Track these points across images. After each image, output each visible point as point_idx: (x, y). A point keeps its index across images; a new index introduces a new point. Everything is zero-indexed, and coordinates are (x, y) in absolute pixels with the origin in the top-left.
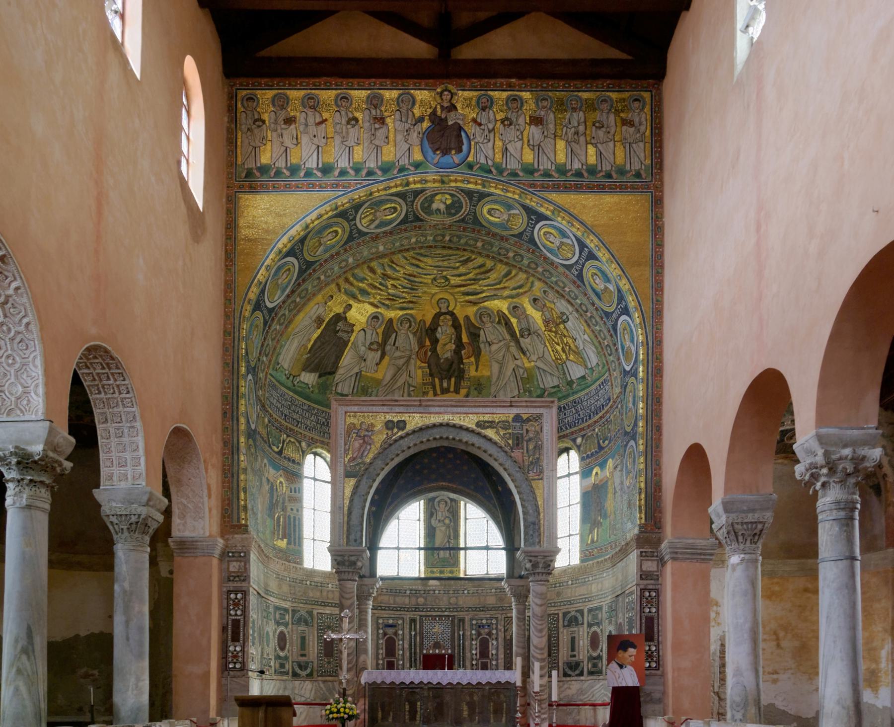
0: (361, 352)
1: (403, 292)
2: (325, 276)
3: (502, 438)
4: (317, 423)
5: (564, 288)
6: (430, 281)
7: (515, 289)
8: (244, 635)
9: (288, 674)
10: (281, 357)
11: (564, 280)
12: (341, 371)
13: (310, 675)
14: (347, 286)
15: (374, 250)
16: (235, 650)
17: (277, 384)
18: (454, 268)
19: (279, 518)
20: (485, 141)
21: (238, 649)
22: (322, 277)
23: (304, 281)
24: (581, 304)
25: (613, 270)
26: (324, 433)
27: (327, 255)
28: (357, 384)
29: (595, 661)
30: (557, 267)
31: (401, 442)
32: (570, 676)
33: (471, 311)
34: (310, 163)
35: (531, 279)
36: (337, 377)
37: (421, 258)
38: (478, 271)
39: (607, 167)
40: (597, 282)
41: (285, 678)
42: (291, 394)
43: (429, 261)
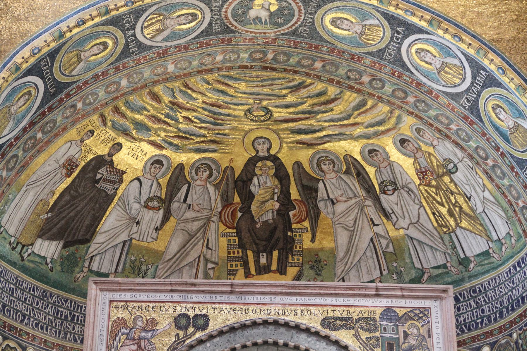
1: (201, 128)
2: (84, 104)
5: (449, 125)
6: (242, 114)
7: (372, 125)
11: (448, 113)
15: (160, 70)
22: (80, 105)
24: (477, 148)
30: (437, 97)
35: (397, 112)
37: (230, 83)
38: (316, 100)
40: (501, 117)
43: (243, 86)
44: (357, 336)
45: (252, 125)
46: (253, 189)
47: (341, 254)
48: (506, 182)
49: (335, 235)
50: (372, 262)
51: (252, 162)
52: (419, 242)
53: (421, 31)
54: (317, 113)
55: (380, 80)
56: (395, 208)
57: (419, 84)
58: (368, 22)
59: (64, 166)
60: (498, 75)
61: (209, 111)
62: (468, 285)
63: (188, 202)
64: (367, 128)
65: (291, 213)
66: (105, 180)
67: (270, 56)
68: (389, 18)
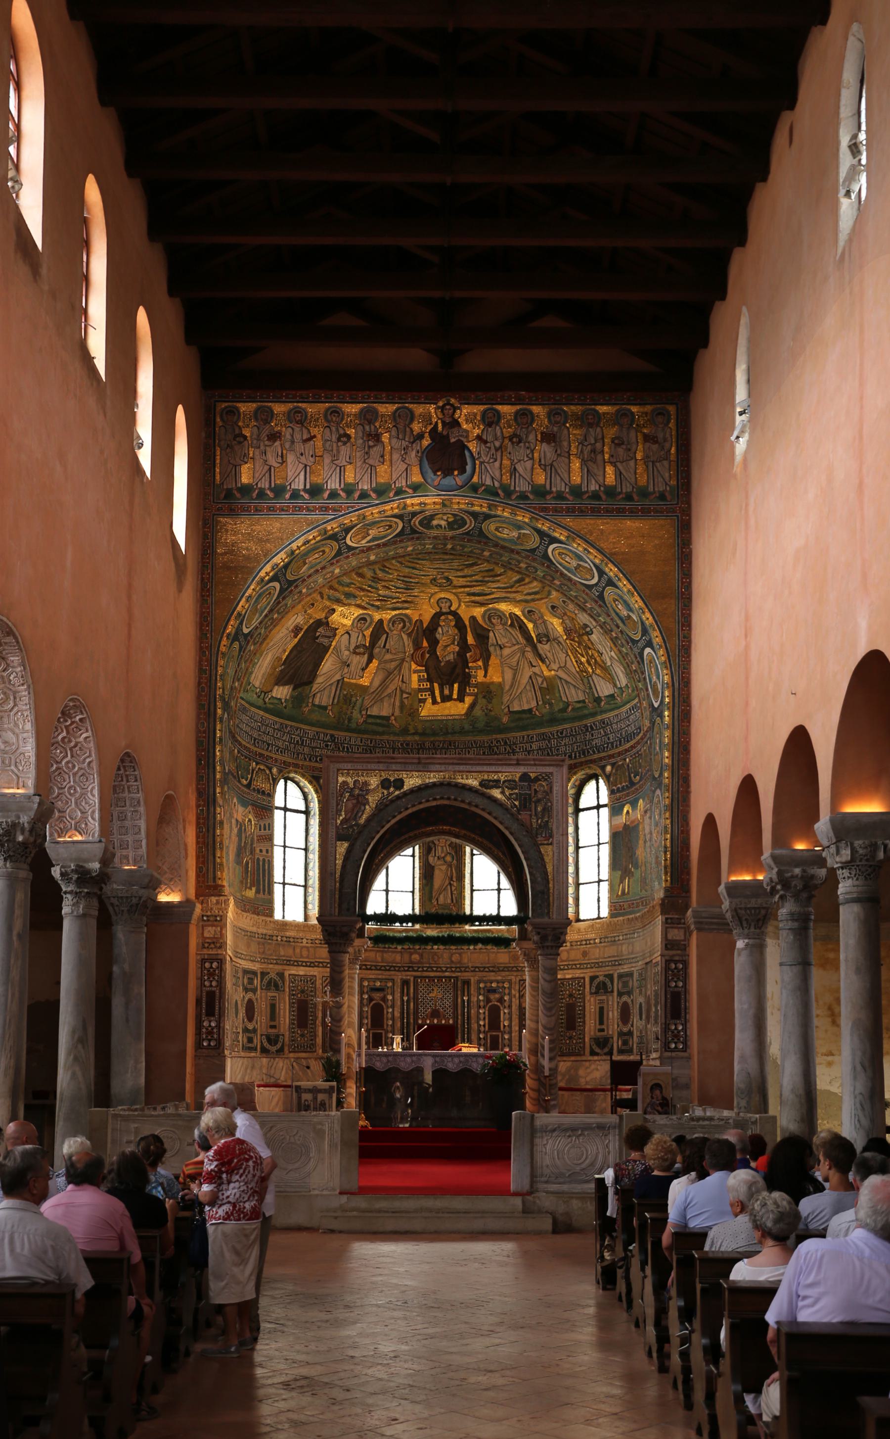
0: (344, 657)
3: (508, 799)
4: (290, 743)
8: (220, 1008)
9: (256, 1049)
10: (253, 675)
11: (584, 596)
12: (319, 680)
15: (364, 560)
16: (210, 1026)
17: (247, 705)
18: (457, 570)
19: (247, 863)
20: (492, 460)
21: (213, 1024)
23: (284, 599)
26: (298, 755)
27: (312, 570)
28: (338, 692)
29: (626, 1037)
31: (399, 802)
32: (597, 1054)
33: (478, 612)
34: (297, 484)
35: (547, 588)
36: (315, 686)
39: (627, 488)
41: (253, 1054)
42: (262, 713)
45: (436, 589)
46: (437, 636)
47: (507, 688)
50: (531, 694)
51: (437, 617)
52: (566, 682)
53: (560, 542)
54: (488, 582)
55: (534, 567)
56: (549, 655)
57: (562, 574)
59: (292, 631)
60: (615, 580)
61: (403, 581)
63: (387, 647)
64: (526, 595)
65: (468, 655)
66: (323, 636)
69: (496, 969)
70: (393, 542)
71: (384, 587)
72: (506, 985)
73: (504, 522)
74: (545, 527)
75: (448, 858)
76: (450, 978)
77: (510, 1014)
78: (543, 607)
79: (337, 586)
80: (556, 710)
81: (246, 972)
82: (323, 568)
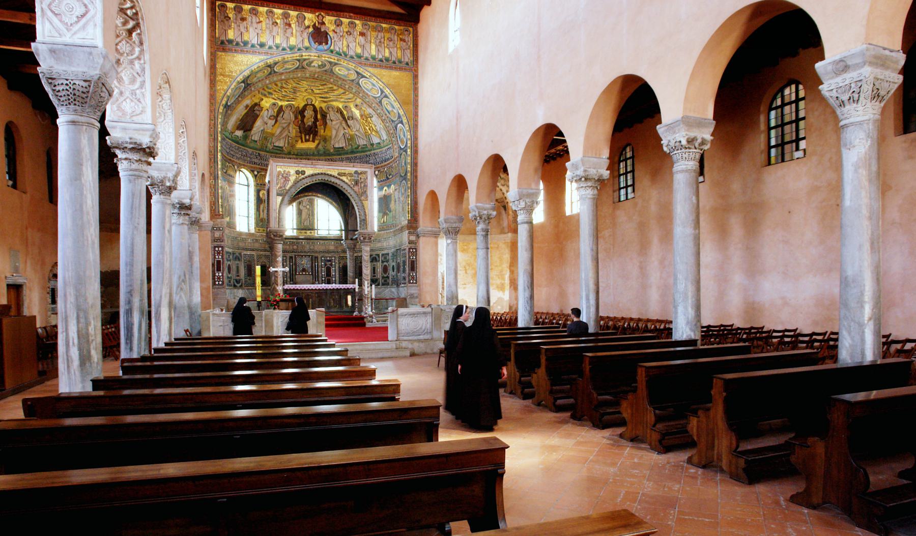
13: (241, 286)
14: (263, 91)
25: (396, 105)
33: (323, 105)
43: (305, 82)
44: (347, 178)
45: (307, 94)
47: (333, 137)
48: (388, 124)
49: (332, 132)
50: (343, 141)
53: (366, 78)
57: (364, 91)
58: (350, 72)
62: (373, 152)
65: (318, 123)
67: (316, 76)
68: (357, 72)
69: (328, 252)
70: (293, 71)
71: (285, 91)
72: (333, 258)
73: (343, 67)
74: (360, 70)
75: (308, 207)
76: (309, 256)
77: (335, 270)
78: (352, 106)
79: (266, 89)
80: (354, 147)
81: (227, 253)
82: (262, 80)
